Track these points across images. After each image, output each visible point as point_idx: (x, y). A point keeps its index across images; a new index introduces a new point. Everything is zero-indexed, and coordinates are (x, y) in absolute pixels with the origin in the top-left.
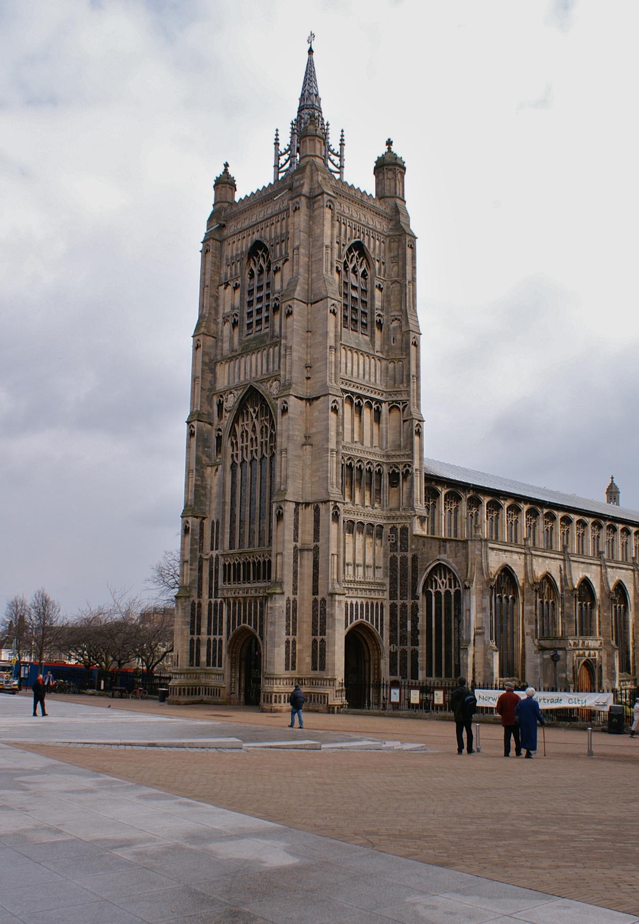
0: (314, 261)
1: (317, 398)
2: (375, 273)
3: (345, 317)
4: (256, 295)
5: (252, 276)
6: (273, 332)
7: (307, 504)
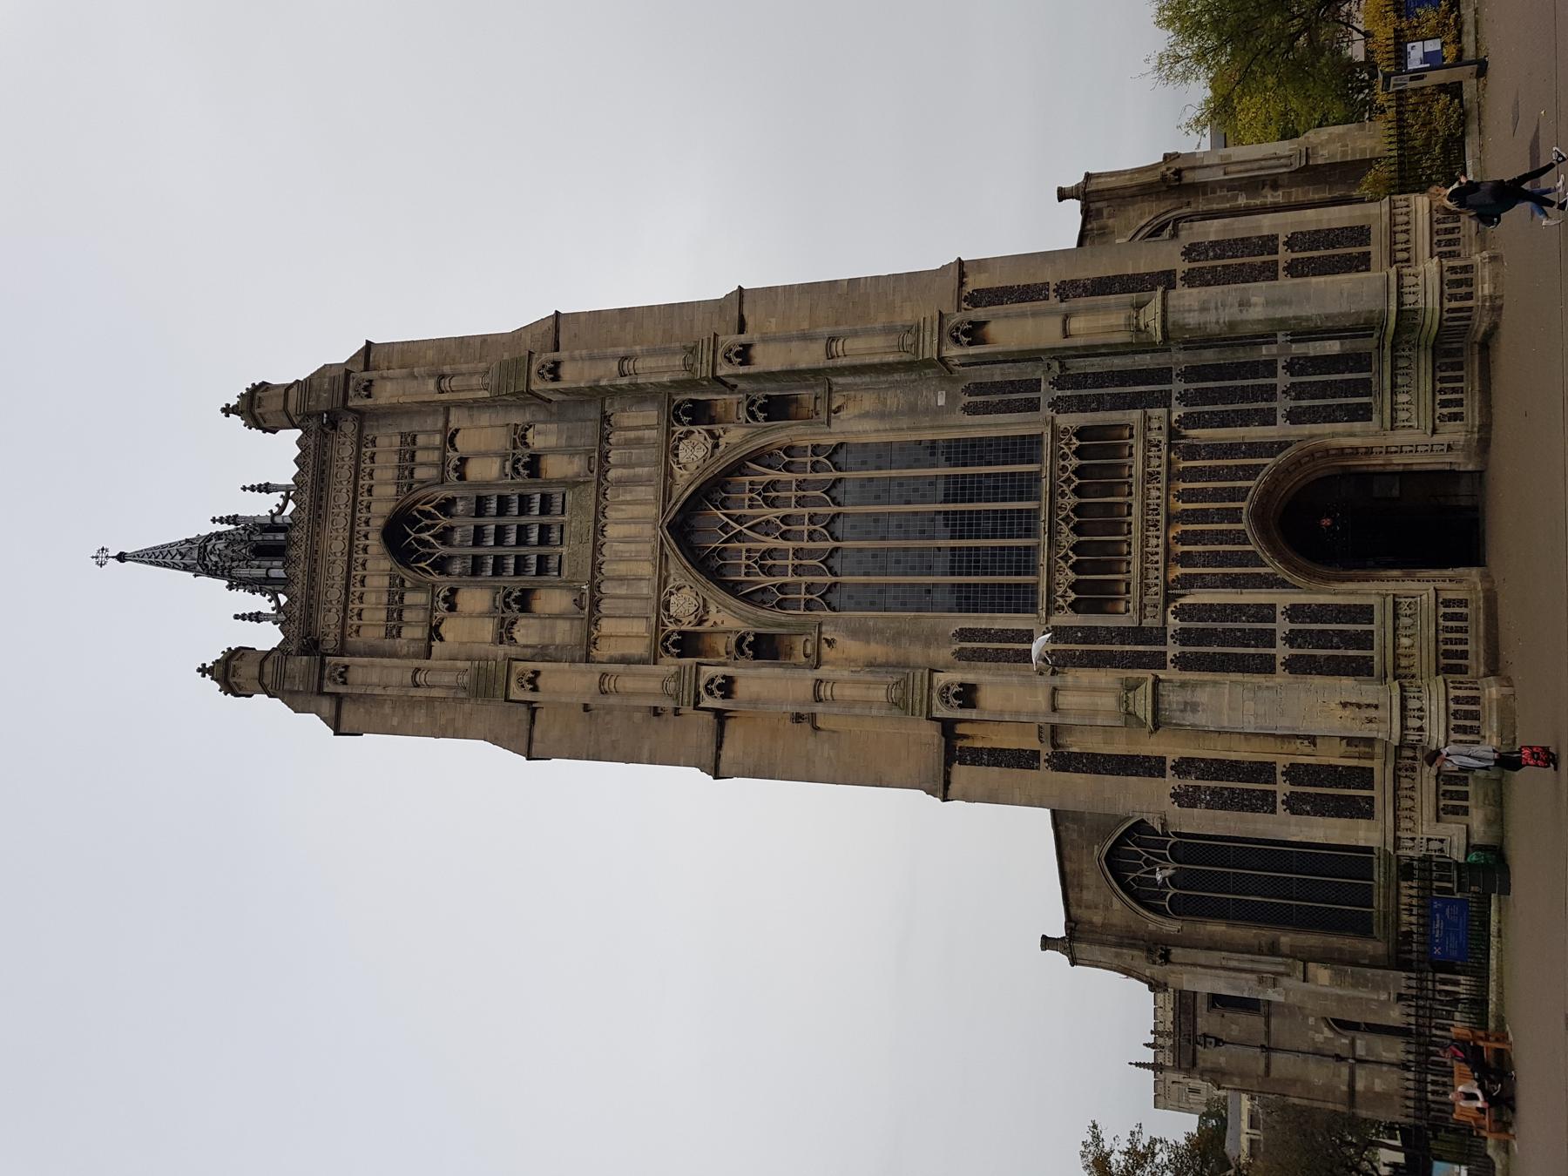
5: (441, 566)
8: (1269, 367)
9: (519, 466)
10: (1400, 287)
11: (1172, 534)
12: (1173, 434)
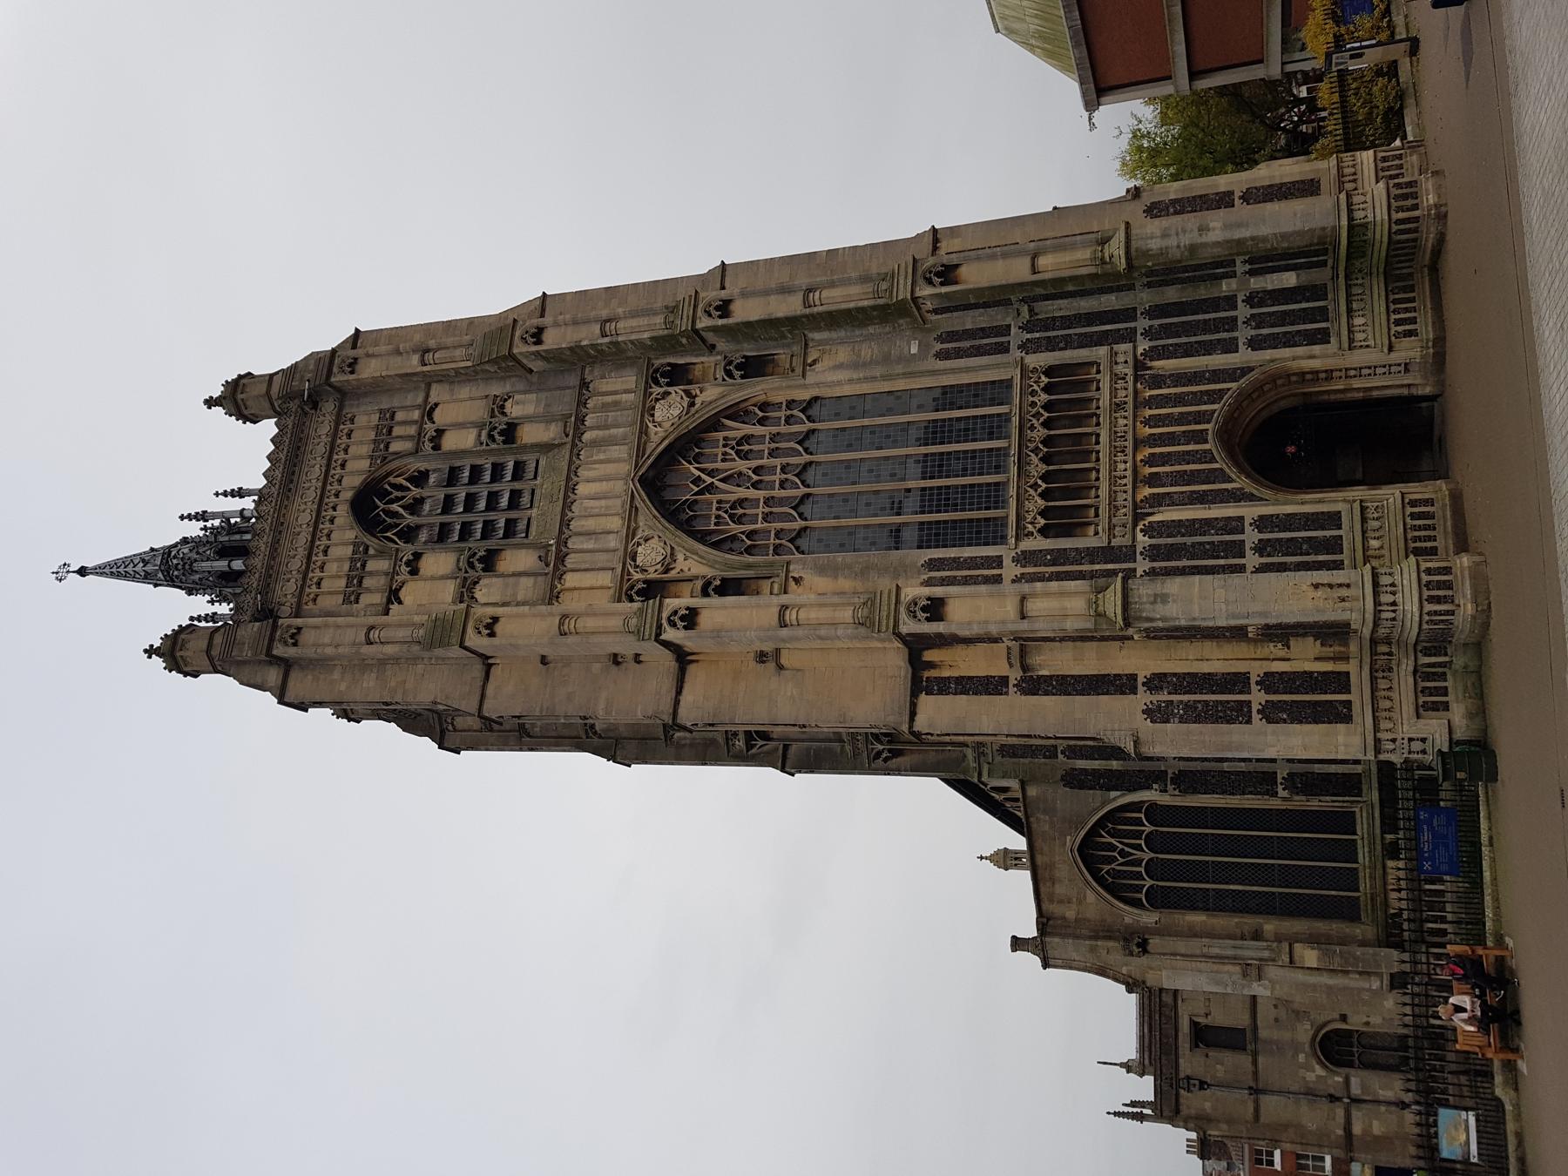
5: (409, 534)
8: (1231, 302)
9: (495, 433)
10: (1349, 204)
11: (1139, 457)
12: (1139, 366)
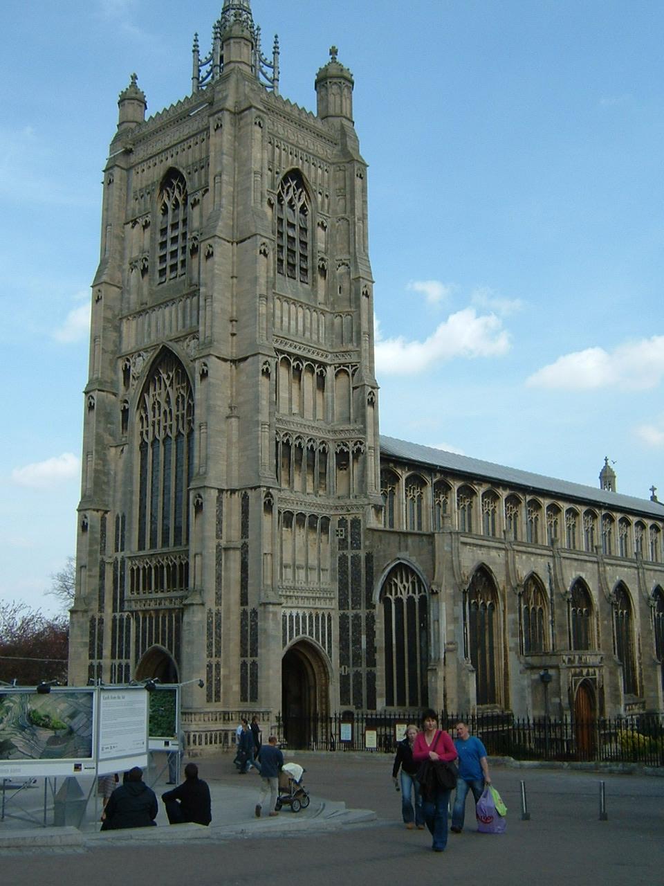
0: (241, 190)
1: (245, 359)
2: (317, 207)
3: (280, 261)
4: (171, 234)
5: (165, 212)
6: (191, 280)
7: (233, 491)
11: (152, 612)
